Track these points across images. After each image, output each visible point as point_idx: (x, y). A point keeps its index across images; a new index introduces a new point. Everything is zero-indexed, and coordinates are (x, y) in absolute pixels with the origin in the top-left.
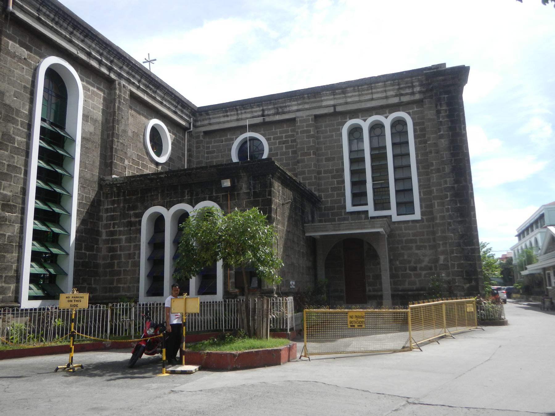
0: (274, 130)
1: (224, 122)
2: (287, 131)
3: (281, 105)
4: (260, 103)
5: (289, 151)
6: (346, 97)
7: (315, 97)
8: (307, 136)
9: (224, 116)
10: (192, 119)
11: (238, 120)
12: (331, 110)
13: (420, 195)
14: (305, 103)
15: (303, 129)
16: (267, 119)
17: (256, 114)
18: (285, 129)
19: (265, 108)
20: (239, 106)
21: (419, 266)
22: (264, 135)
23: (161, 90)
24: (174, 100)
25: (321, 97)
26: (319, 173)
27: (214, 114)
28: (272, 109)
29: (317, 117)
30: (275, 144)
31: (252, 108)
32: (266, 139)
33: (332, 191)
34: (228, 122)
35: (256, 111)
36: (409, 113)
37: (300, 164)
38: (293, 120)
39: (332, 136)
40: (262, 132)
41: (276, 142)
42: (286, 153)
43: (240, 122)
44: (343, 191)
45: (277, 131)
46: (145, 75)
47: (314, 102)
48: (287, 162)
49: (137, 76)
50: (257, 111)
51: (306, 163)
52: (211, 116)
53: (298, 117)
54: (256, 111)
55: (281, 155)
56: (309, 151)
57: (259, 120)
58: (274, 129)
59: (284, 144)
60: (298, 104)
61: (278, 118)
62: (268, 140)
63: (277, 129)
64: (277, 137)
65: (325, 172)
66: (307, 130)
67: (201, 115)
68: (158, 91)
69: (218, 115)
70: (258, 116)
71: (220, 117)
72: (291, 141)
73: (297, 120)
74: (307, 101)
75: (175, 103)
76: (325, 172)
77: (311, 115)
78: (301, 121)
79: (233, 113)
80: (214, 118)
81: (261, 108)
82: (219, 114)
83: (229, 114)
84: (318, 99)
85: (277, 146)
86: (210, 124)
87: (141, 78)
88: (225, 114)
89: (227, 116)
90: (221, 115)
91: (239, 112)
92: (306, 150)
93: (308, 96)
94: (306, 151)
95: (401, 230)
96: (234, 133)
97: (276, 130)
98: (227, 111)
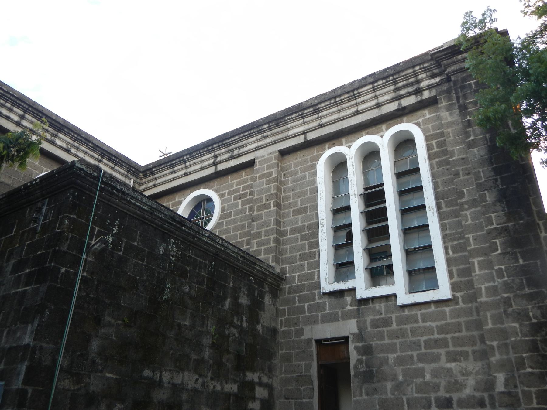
0: (229, 182)
1: (170, 181)
2: (246, 181)
3: (237, 145)
4: (211, 147)
5: (246, 208)
6: (320, 118)
7: (278, 125)
8: (267, 180)
9: (171, 173)
10: (132, 181)
11: (186, 174)
12: (301, 140)
13: (447, 253)
14: (267, 137)
15: (263, 173)
16: (221, 167)
17: (206, 163)
18: (244, 178)
19: (217, 153)
20: (186, 155)
21: (455, 397)
22: (217, 191)
23: (66, 134)
24: (94, 151)
25: (286, 124)
26: (283, 234)
27: (160, 172)
28: (226, 152)
29: (284, 153)
30: (229, 200)
31: (201, 155)
32: (219, 195)
33: (301, 260)
34: (175, 179)
35: (207, 160)
36: (418, 124)
37: (255, 223)
38: (250, 164)
39: (304, 177)
40: (216, 187)
41: (231, 198)
42: (242, 211)
43: (189, 176)
44: (317, 259)
45: (233, 183)
46: (30, 109)
47: (278, 133)
48: (242, 223)
49: (15, 109)
50: (208, 159)
51: (263, 220)
52: (156, 176)
53: (258, 158)
54: (207, 160)
55: (235, 215)
56: (269, 202)
57: (211, 171)
58: (230, 180)
59: (240, 198)
60: (258, 140)
61: (233, 163)
62: (221, 196)
63: (233, 180)
64: (233, 191)
65: (293, 231)
66: (268, 172)
67: (145, 176)
68: (60, 135)
69: (164, 173)
70: (209, 166)
71: (166, 175)
72: (250, 193)
73: (257, 162)
74: (269, 133)
75: (96, 156)
76: (293, 231)
77: (275, 152)
78: (261, 163)
79: (180, 167)
80: (160, 177)
81: (213, 154)
82: (165, 170)
83: (176, 169)
84: (282, 128)
85: (231, 203)
86: (155, 186)
87: (25, 112)
88: (171, 170)
89: (174, 172)
90: (168, 171)
91: (188, 164)
92: (264, 200)
93: (269, 126)
94: (264, 203)
95: (417, 321)
96: (183, 195)
97: (233, 182)
98: (173, 166)
